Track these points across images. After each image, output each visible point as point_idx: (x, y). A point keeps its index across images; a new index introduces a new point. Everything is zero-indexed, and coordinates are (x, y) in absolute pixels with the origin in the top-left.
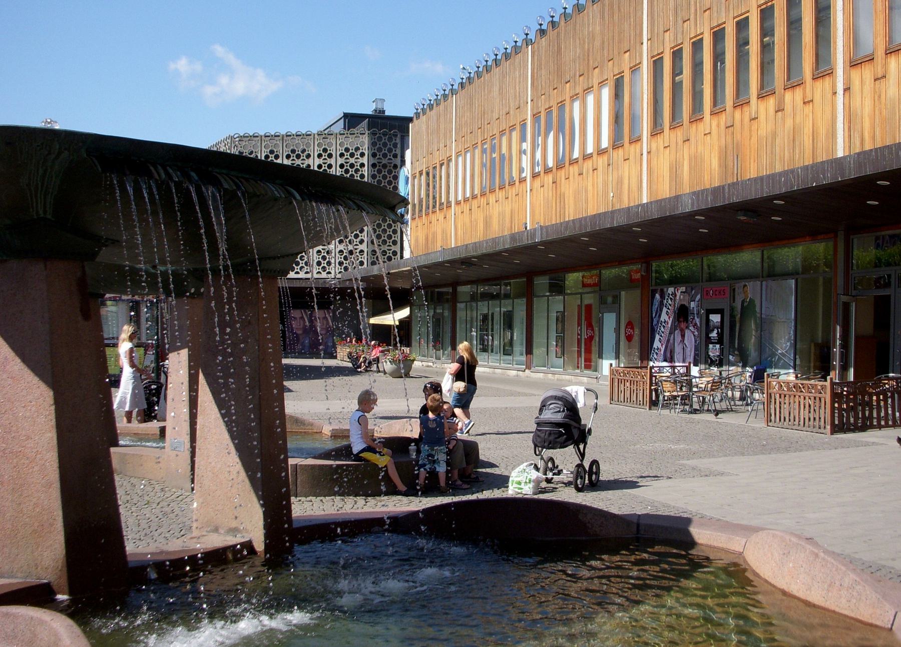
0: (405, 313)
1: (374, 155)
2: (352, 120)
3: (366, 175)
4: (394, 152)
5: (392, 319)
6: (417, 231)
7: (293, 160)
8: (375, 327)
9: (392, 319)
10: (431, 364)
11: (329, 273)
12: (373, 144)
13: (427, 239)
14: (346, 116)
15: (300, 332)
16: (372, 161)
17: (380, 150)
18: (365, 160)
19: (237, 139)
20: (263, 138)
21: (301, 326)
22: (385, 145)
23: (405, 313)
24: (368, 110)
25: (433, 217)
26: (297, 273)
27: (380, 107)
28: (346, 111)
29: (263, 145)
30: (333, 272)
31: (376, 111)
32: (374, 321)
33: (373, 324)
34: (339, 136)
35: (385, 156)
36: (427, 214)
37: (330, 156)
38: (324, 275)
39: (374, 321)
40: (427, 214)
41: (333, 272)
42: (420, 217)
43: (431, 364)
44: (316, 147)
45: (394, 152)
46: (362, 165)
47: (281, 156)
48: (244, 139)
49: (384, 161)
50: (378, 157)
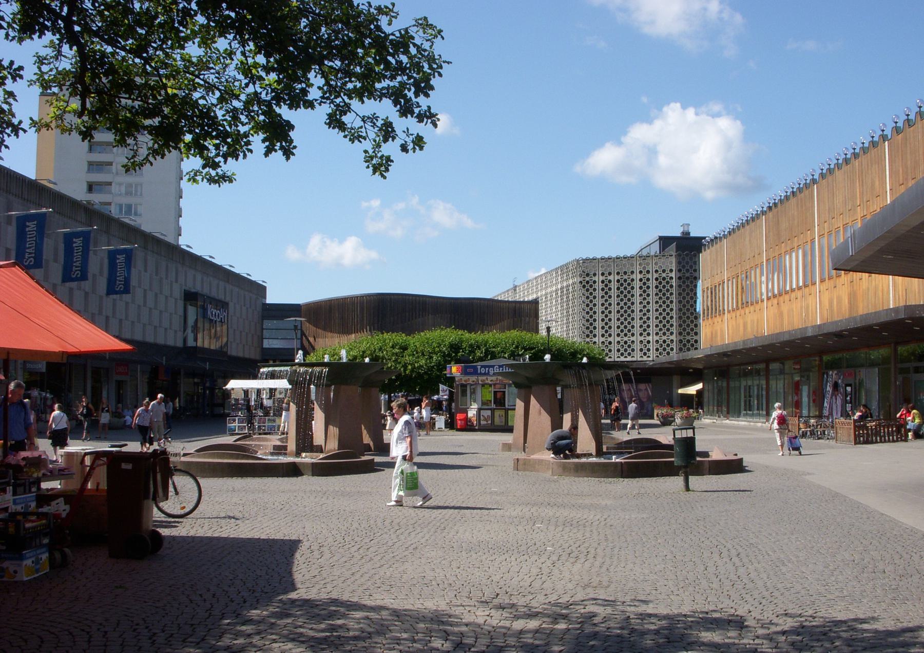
0: (700, 386)
1: (680, 271)
2: (665, 241)
3: (674, 285)
4: (694, 268)
5: (692, 390)
6: (706, 328)
7: (622, 276)
8: (683, 395)
9: (692, 390)
10: (715, 421)
11: (649, 357)
12: (679, 263)
13: (712, 334)
14: (661, 238)
15: (645, 400)
16: (678, 275)
17: (684, 267)
18: (673, 275)
19: (581, 262)
20: (600, 260)
21: (646, 396)
22: (687, 263)
23: (700, 386)
24: (677, 233)
25: (715, 320)
26: (626, 357)
27: (686, 229)
28: (660, 235)
29: (600, 265)
30: (651, 356)
31: (683, 233)
32: (680, 391)
33: (681, 394)
34: (654, 258)
35: (687, 271)
36: (712, 318)
37: (648, 272)
38: (645, 358)
39: (680, 391)
40: (712, 318)
41: (651, 356)
42: (708, 319)
43: (715, 421)
44: (638, 266)
45: (694, 268)
46: (671, 278)
47: (613, 273)
48: (586, 261)
49: (688, 275)
50: (683, 272)
